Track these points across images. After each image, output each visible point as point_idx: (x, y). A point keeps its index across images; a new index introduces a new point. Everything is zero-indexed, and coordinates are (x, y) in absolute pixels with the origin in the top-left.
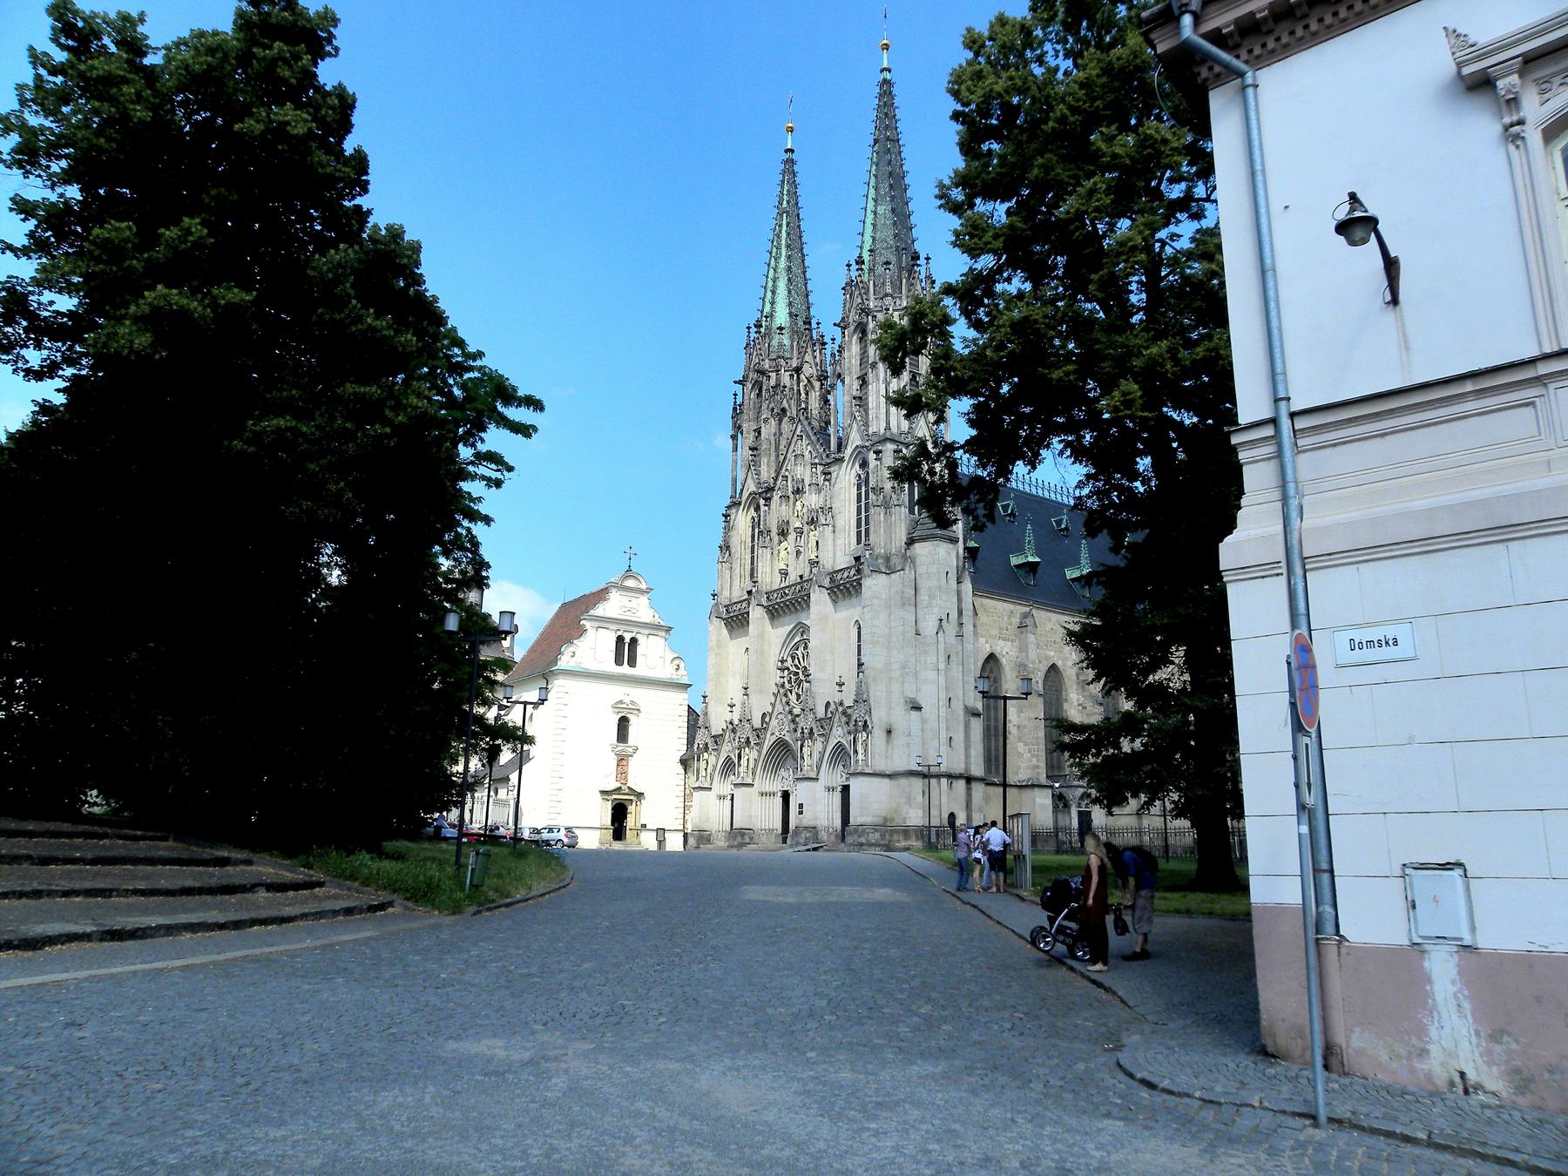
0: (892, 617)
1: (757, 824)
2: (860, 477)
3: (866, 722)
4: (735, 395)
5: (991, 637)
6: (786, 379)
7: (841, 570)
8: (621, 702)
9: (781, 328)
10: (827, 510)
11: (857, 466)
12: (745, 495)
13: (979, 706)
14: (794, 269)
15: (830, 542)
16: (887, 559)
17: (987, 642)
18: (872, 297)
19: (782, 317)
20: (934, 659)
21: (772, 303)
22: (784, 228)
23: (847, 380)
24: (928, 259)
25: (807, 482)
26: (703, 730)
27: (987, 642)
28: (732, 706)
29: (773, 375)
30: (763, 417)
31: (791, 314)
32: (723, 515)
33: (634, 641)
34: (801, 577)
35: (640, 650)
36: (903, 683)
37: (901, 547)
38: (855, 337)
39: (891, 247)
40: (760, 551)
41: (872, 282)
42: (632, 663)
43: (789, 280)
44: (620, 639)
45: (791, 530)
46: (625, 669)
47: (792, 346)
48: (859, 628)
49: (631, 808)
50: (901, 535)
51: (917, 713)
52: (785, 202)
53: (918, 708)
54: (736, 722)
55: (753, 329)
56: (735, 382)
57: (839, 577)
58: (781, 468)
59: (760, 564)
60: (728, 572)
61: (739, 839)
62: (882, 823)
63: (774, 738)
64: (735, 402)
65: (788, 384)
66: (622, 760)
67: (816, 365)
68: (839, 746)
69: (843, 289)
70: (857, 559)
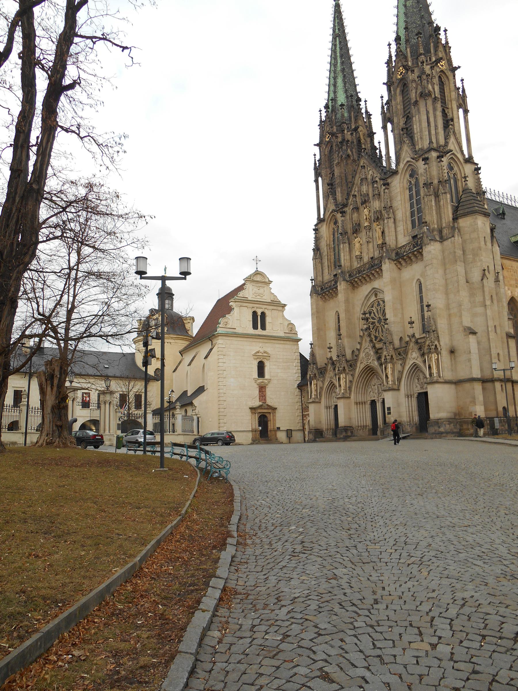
0: (448, 271)
1: (355, 423)
2: (410, 182)
3: (436, 346)
4: (315, 155)
5: (511, 285)
6: (348, 135)
7: (403, 246)
8: (258, 352)
9: (342, 105)
10: (389, 208)
11: (408, 176)
12: (328, 214)
13: (512, 331)
14: (346, 70)
15: (393, 229)
16: (440, 231)
17: (509, 289)
18: (410, 59)
19: (341, 98)
20: (481, 299)
21: (335, 92)
22: (338, 46)
23: (395, 120)
24: (445, 31)
25: (371, 195)
26: (312, 365)
27: (509, 289)
28: (330, 348)
29: (339, 135)
30: (335, 163)
31: (347, 97)
32: (314, 230)
33: (263, 314)
34: (372, 258)
35: (268, 320)
36: (461, 316)
37: (449, 222)
38: (398, 90)
39: (419, 26)
40: (342, 246)
41: (408, 50)
42: (263, 328)
43: (344, 76)
44: (255, 314)
45: (362, 228)
46: (259, 331)
47: (350, 117)
48: (420, 285)
49: (271, 417)
50: (448, 213)
51: (474, 336)
52: (337, 31)
53: (474, 333)
54: (335, 358)
55: (324, 110)
56: (315, 145)
57: (403, 250)
58: (351, 191)
59: (342, 255)
60: (320, 265)
61: (344, 434)
62: (453, 417)
63: (362, 366)
64: (315, 160)
65: (350, 139)
66: (262, 389)
67: (366, 127)
68: (415, 367)
69: (386, 63)
70: (414, 237)
